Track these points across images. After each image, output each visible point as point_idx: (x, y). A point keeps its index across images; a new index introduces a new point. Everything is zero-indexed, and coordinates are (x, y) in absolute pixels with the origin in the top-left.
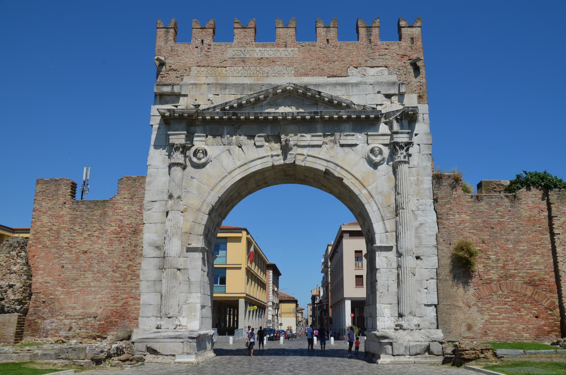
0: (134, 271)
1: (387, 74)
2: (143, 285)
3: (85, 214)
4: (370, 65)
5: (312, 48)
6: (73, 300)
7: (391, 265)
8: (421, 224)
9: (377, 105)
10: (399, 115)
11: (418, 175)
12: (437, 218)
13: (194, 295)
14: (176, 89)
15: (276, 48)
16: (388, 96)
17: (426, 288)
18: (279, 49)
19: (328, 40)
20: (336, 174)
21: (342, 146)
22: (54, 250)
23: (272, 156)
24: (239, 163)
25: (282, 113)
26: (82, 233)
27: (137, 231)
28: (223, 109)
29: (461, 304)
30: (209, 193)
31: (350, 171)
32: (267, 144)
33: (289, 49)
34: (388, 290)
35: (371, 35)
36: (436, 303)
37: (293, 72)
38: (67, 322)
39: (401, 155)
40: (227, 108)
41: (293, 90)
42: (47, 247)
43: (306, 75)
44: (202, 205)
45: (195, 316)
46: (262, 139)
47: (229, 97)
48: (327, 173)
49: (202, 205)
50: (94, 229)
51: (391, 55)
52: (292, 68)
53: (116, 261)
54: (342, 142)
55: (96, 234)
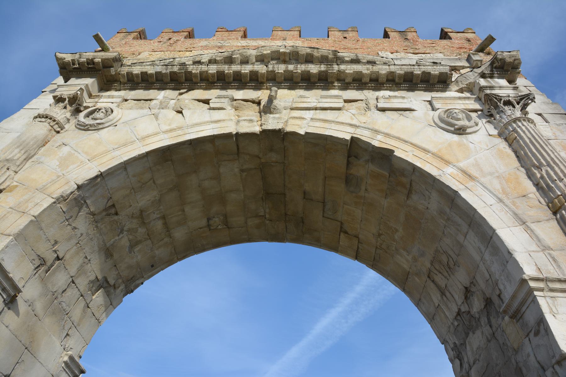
20: (376, 144)
21: (383, 110)
31: (407, 139)
41: (290, 53)
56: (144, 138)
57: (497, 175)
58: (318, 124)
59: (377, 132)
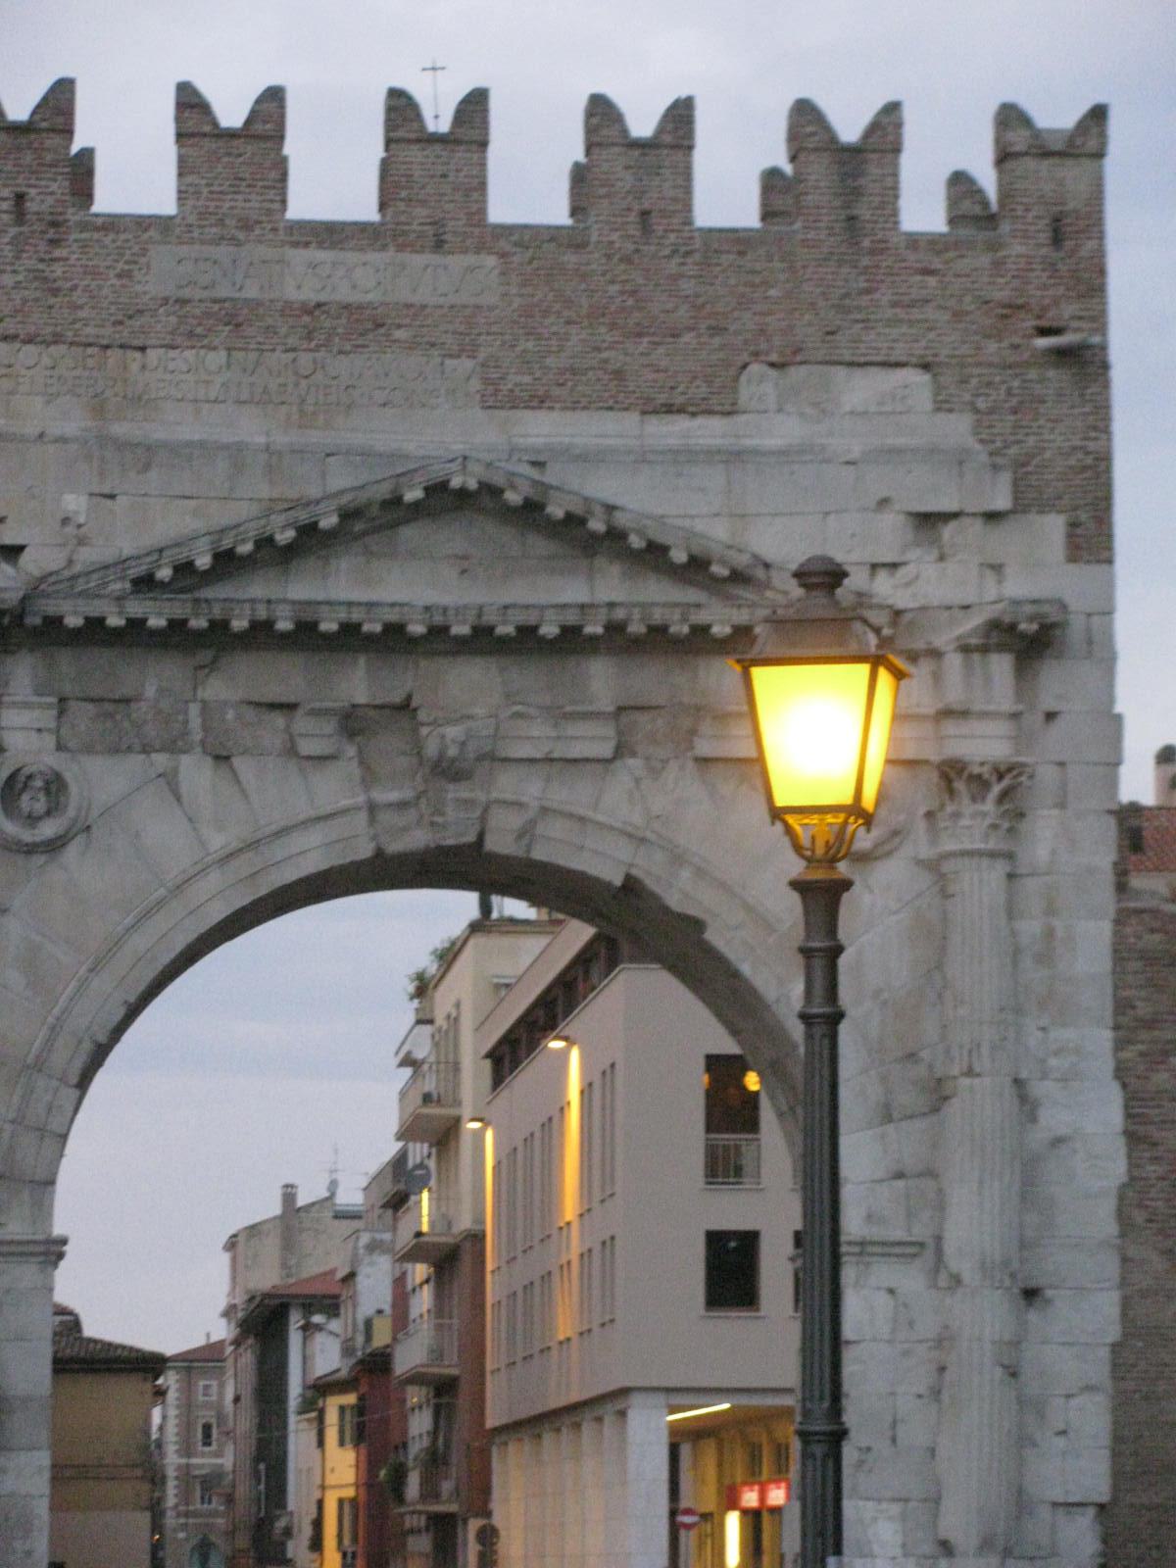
1: (929, 406)
4: (848, 358)
5: (570, 259)
7: (911, 1324)
8: (1058, 1141)
9: (874, 567)
10: (974, 631)
11: (1051, 911)
12: (1129, 1116)
13: (23, 1458)
15: (390, 254)
16: (928, 522)
17: (1063, 1433)
18: (406, 257)
19: (645, 214)
20: (674, 901)
21: (704, 761)
23: (372, 808)
24: (217, 842)
25: (427, 608)
28: (145, 583)
30: (84, 983)
32: (351, 751)
33: (457, 262)
34: (894, 1440)
35: (857, 193)
36: (1105, 1498)
37: (475, 384)
39: (973, 823)
40: (165, 573)
41: (479, 492)
43: (540, 401)
44: (49, 1043)
45: (29, 1553)
46: (329, 726)
47: (169, 520)
48: (631, 887)
49: (49, 1043)
51: (952, 303)
52: (468, 364)
54: (704, 748)
56: (179, 888)
57: (886, 995)
58: (555, 828)
59: (678, 858)
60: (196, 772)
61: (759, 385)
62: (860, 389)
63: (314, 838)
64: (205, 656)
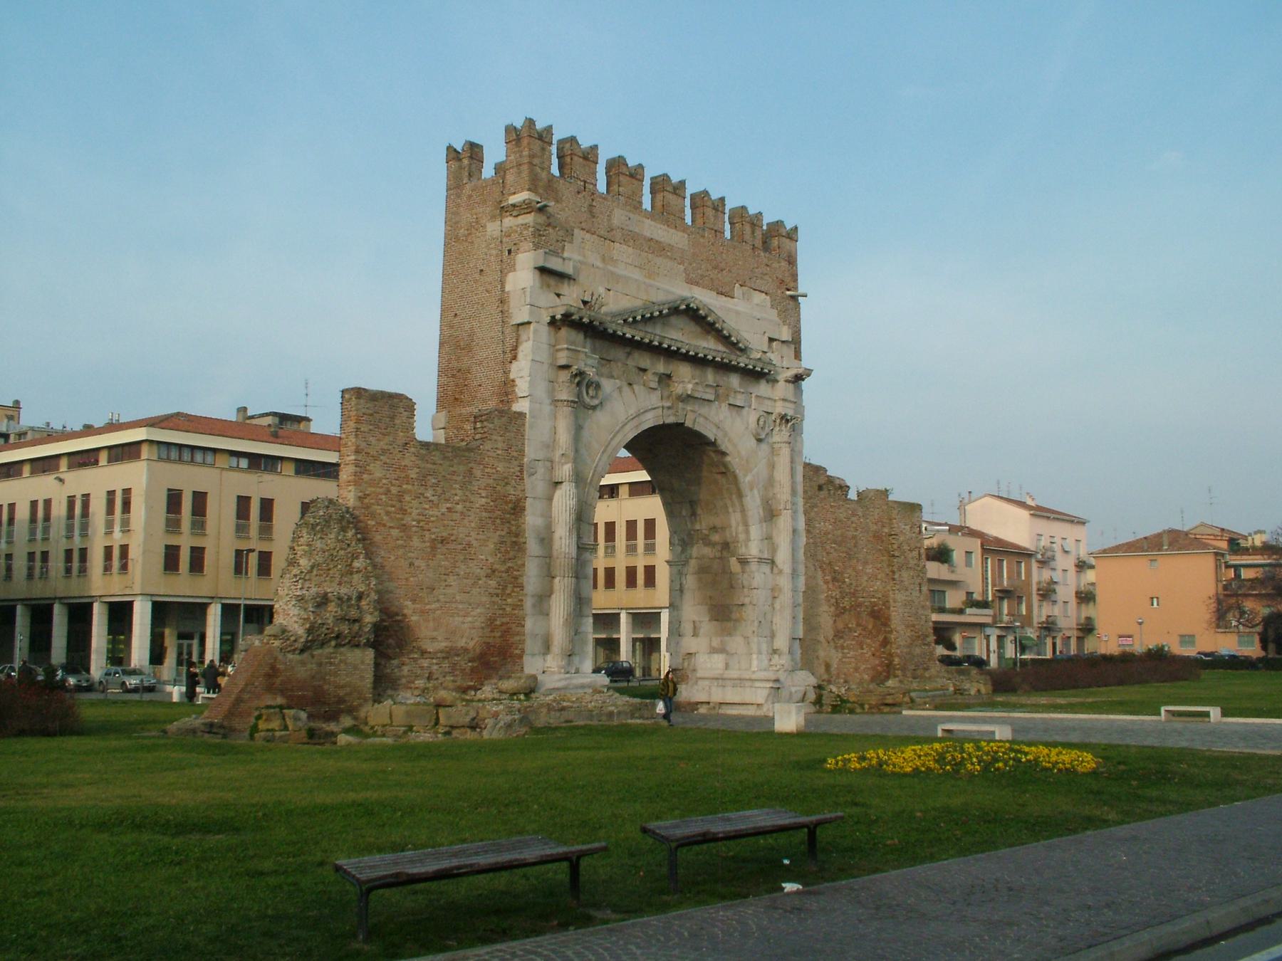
0: (516, 578)
2: (528, 603)
3: (441, 469)
6: (431, 624)
14: (568, 269)
22: (395, 532)
26: (437, 506)
27: (518, 509)
29: (822, 639)
38: (425, 663)
42: (384, 525)
43: (697, 284)
50: (457, 498)
53: (491, 560)
55: (459, 507)
58: (701, 420)
59: (726, 434)
60: (626, 389)
61: (738, 290)
62: (759, 298)
63: (650, 415)
64: (628, 350)
